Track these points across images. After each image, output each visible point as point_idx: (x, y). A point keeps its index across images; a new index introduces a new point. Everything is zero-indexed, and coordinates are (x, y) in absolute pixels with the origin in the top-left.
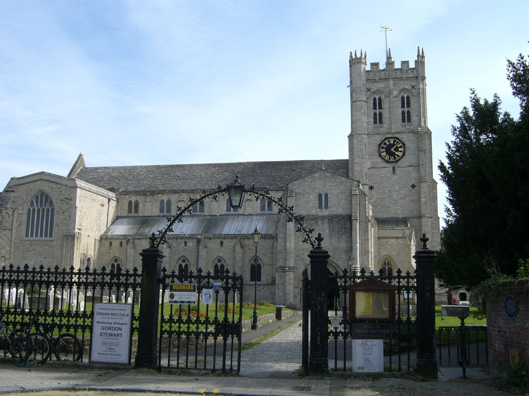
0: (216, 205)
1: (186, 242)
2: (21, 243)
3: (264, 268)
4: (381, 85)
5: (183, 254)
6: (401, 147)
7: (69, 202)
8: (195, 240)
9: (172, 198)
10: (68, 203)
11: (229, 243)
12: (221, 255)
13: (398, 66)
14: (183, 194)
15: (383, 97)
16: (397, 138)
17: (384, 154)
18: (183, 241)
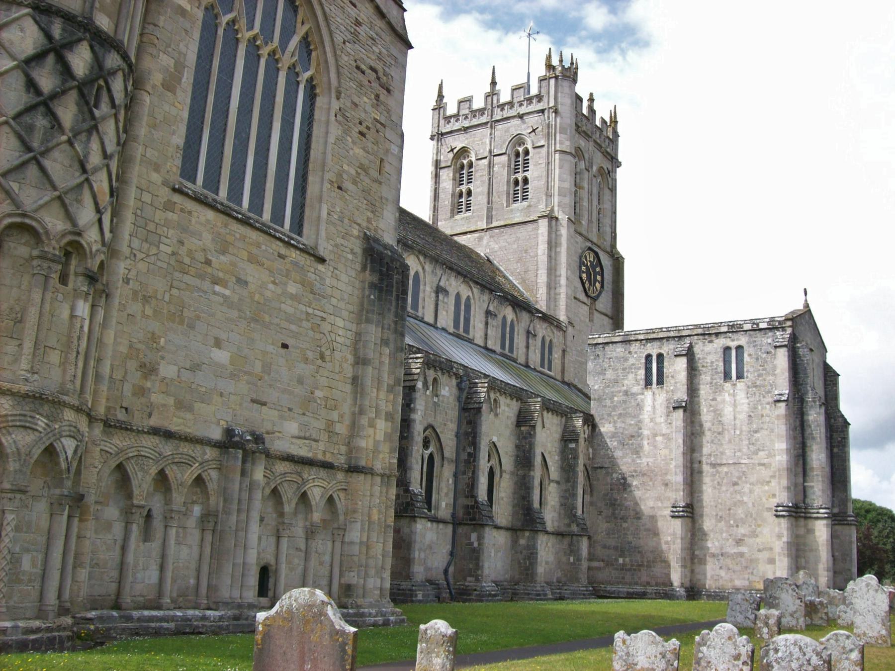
2: (169, 206)
4: (582, 143)
7: (383, 93)
8: (454, 382)
10: (377, 97)
11: (507, 409)
12: (495, 439)
13: (598, 123)
16: (596, 254)
17: (584, 276)
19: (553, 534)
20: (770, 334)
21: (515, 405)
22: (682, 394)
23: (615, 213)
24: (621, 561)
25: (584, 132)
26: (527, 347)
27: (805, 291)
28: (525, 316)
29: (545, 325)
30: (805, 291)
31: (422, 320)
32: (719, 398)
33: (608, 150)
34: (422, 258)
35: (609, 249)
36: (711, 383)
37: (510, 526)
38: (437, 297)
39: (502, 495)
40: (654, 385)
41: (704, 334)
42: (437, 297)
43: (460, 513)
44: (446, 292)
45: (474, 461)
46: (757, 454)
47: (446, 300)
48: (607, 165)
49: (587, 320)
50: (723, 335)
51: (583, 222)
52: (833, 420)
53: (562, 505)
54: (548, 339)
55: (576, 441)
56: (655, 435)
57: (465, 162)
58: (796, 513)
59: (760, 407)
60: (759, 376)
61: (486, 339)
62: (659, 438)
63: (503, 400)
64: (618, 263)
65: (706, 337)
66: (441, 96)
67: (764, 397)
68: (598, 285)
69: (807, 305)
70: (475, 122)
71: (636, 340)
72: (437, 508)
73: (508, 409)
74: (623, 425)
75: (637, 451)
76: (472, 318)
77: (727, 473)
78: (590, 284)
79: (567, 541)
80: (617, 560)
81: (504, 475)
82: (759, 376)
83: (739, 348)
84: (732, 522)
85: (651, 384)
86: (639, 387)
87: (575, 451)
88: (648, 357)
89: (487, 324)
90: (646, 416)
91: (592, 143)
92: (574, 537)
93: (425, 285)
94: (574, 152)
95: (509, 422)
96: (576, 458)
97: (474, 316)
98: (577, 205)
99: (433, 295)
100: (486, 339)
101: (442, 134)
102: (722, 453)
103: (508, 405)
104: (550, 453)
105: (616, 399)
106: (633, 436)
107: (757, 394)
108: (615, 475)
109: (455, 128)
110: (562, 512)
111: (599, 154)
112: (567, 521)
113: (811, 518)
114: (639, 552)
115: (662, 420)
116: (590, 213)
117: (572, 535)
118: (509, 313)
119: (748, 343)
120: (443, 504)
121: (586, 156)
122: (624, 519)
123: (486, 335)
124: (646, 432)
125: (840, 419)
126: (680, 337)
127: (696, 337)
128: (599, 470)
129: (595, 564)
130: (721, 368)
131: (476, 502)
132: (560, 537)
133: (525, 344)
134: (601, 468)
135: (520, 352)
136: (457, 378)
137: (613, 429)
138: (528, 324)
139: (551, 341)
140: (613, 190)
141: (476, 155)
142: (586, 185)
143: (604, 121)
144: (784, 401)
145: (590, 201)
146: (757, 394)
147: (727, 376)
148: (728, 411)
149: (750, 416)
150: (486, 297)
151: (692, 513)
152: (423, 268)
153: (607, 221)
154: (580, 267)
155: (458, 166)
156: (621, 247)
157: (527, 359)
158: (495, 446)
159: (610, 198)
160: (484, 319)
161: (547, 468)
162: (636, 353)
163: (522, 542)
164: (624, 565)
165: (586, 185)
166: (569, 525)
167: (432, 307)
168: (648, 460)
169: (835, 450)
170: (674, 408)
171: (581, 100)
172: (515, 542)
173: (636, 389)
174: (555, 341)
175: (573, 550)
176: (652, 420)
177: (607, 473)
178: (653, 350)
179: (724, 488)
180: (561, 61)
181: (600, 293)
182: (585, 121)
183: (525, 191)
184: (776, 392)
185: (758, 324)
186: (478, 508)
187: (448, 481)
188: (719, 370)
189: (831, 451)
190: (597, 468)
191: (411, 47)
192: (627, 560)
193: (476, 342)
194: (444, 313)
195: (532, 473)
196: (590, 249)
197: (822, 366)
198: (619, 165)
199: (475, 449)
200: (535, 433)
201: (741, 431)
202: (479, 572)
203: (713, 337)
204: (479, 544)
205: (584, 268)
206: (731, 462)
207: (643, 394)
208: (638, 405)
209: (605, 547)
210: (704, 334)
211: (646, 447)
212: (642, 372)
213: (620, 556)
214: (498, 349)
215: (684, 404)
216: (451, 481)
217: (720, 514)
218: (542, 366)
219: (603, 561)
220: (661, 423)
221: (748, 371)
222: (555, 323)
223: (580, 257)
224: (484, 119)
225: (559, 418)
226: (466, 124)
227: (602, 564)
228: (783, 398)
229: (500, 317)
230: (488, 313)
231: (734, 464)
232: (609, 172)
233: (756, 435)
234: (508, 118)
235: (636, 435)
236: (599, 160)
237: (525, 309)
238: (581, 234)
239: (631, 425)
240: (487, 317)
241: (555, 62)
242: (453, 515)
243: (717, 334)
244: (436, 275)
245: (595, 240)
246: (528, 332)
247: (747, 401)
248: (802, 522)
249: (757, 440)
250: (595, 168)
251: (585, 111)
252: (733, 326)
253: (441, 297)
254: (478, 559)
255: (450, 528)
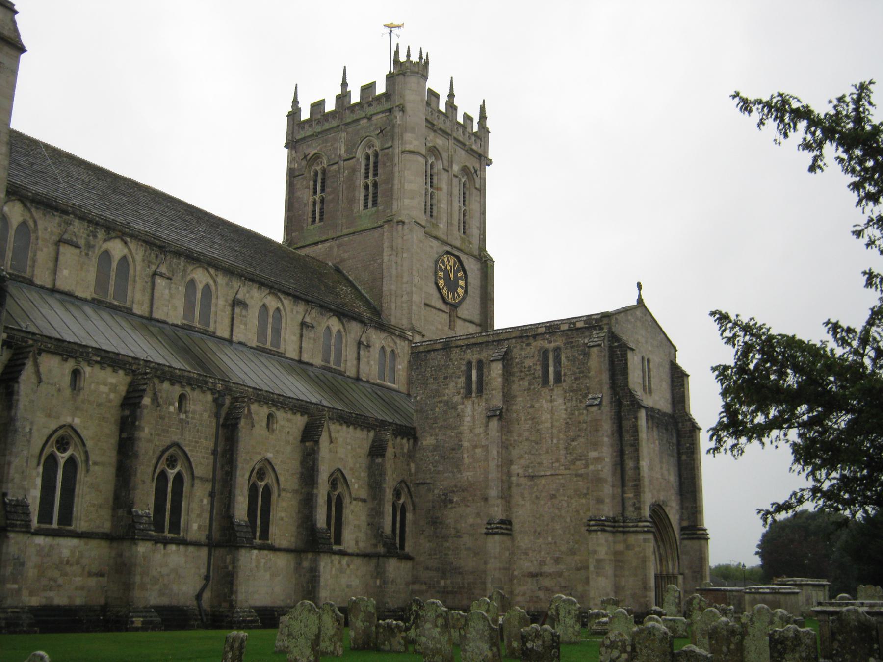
0: (167, 292)
1: (182, 398)
3: (352, 507)
4: (440, 142)
5: (175, 438)
6: (461, 278)
8: (209, 397)
9: (41, 224)
11: (287, 424)
12: (269, 455)
13: (460, 119)
14: (77, 222)
15: (439, 165)
16: (458, 258)
17: (441, 282)
18: (177, 390)
19: (358, 555)
20: (587, 334)
21: (300, 421)
22: (497, 401)
23: (484, 213)
24: (442, 583)
25: (440, 129)
26: (358, 359)
27: (639, 286)
28: (355, 328)
29: (383, 335)
30: (639, 286)
31: (213, 335)
32: (537, 406)
33: (474, 147)
34: (212, 271)
35: (476, 253)
36: (529, 389)
37: (293, 547)
38: (233, 310)
39: (283, 515)
40: (474, 395)
41: (521, 337)
42: (233, 310)
43: (216, 535)
44: (244, 304)
45: (231, 479)
46: (574, 464)
47: (244, 312)
48: (472, 163)
49: (446, 328)
50: (540, 337)
51: (441, 226)
52: (680, 425)
53: (369, 525)
54: (388, 350)
55: (383, 456)
56: (475, 447)
57: (318, 168)
58: (614, 527)
59: (577, 413)
60: (576, 379)
61: (301, 352)
62: (478, 451)
63: (280, 415)
64: (486, 265)
65: (524, 340)
66: (295, 102)
67: (581, 402)
68: (460, 291)
69: (640, 301)
70: (327, 126)
71: (457, 347)
72: (187, 530)
73: (291, 425)
74: (444, 438)
75: (458, 465)
76: (283, 331)
77: (544, 485)
78: (449, 289)
79: (374, 561)
80: (438, 582)
81: (283, 494)
82: (576, 379)
83: (557, 350)
84: (550, 539)
85: (471, 393)
86: (459, 396)
87: (381, 466)
88: (469, 364)
89: (301, 336)
90: (465, 428)
91: (451, 142)
92: (381, 559)
93: (217, 298)
94: (423, 151)
95: (291, 438)
96: (382, 474)
97: (286, 329)
98: (434, 208)
99: (229, 309)
100: (301, 352)
101: (297, 141)
102: (540, 464)
103: (289, 420)
104: (352, 469)
105: (437, 409)
106: (453, 449)
107: (574, 398)
108: (436, 492)
109: (308, 134)
110: (369, 532)
111: (463, 152)
112: (374, 541)
113: (629, 532)
114: (460, 573)
115: (481, 430)
116: (450, 215)
117: (378, 556)
118: (334, 324)
119: (565, 344)
120: (195, 526)
121: (445, 155)
122: (445, 538)
123: (301, 348)
124: (466, 444)
125: (688, 423)
126: (499, 341)
127: (514, 341)
128: (421, 486)
129: (416, 587)
130: (539, 373)
131: (232, 523)
132: (367, 559)
133: (355, 355)
134: (423, 484)
135: (349, 364)
136: (213, 394)
137: (434, 442)
138: (359, 334)
139: (393, 351)
140: (482, 190)
141: (329, 160)
142: (444, 187)
143: (467, 118)
144: (596, 405)
145: (450, 203)
146: (574, 398)
147: (545, 382)
148: (546, 416)
149: (567, 423)
150: (301, 308)
151: (510, 530)
152: (215, 282)
153: (474, 224)
154: (436, 273)
155: (312, 173)
156: (491, 249)
157: (358, 372)
158: (270, 464)
159: (478, 198)
160: (298, 332)
161: (348, 486)
162: (456, 360)
163: (306, 564)
164: (445, 587)
165: (444, 187)
166: (375, 546)
167: (227, 321)
168: (468, 474)
169: (684, 457)
170: (489, 417)
171: (437, 96)
172: (299, 564)
173: (457, 398)
174: (398, 351)
175: (379, 573)
176: (471, 431)
177: (429, 490)
178: (473, 356)
179: (542, 502)
180: (408, 56)
181: (463, 299)
182: (442, 118)
183: (375, 196)
184: (590, 396)
185: (574, 324)
186: (233, 529)
187: (202, 501)
188: (536, 375)
189: (679, 458)
190: (419, 484)
191: (22, 50)
192: (449, 582)
193: (287, 355)
194: (242, 327)
195: (315, 491)
196: (448, 253)
197: (667, 366)
198: (489, 163)
199: (231, 468)
200: (319, 448)
201: (559, 440)
202: (233, 597)
203: (531, 340)
204: (233, 568)
205: (440, 274)
206: (549, 473)
207: (463, 404)
208: (458, 415)
209: (427, 568)
210: (521, 337)
211: (466, 461)
212: (462, 380)
213: (442, 578)
214: (318, 361)
215: (498, 413)
216: (205, 501)
217: (538, 529)
218: (382, 375)
219: (425, 583)
220: (480, 434)
221: (565, 375)
222: (397, 333)
223: (436, 262)
224: (334, 123)
225: (365, 432)
226: (318, 129)
227: (424, 587)
228: (596, 402)
229: (321, 329)
230: (303, 324)
231: (552, 475)
232: (476, 171)
233: (574, 444)
234: (358, 120)
235: (458, 447)
236: (461, 158)
237: (354, 319)
238: (436, 238)
239: (451, 437)
240: (302, 329)
241: (403, 58)
242: (209, 537)
243: (535, 337)
244: (232, 287)
245: (458, 243)
246: (360, 343)
247: (564, 407)
248: (620, 537)
249: (575, 448)
250: (456, 168)
251: (442, 107)
252: (550, 327)
253: (237, 310)
254: (231, 583)
255: (204, 552)
